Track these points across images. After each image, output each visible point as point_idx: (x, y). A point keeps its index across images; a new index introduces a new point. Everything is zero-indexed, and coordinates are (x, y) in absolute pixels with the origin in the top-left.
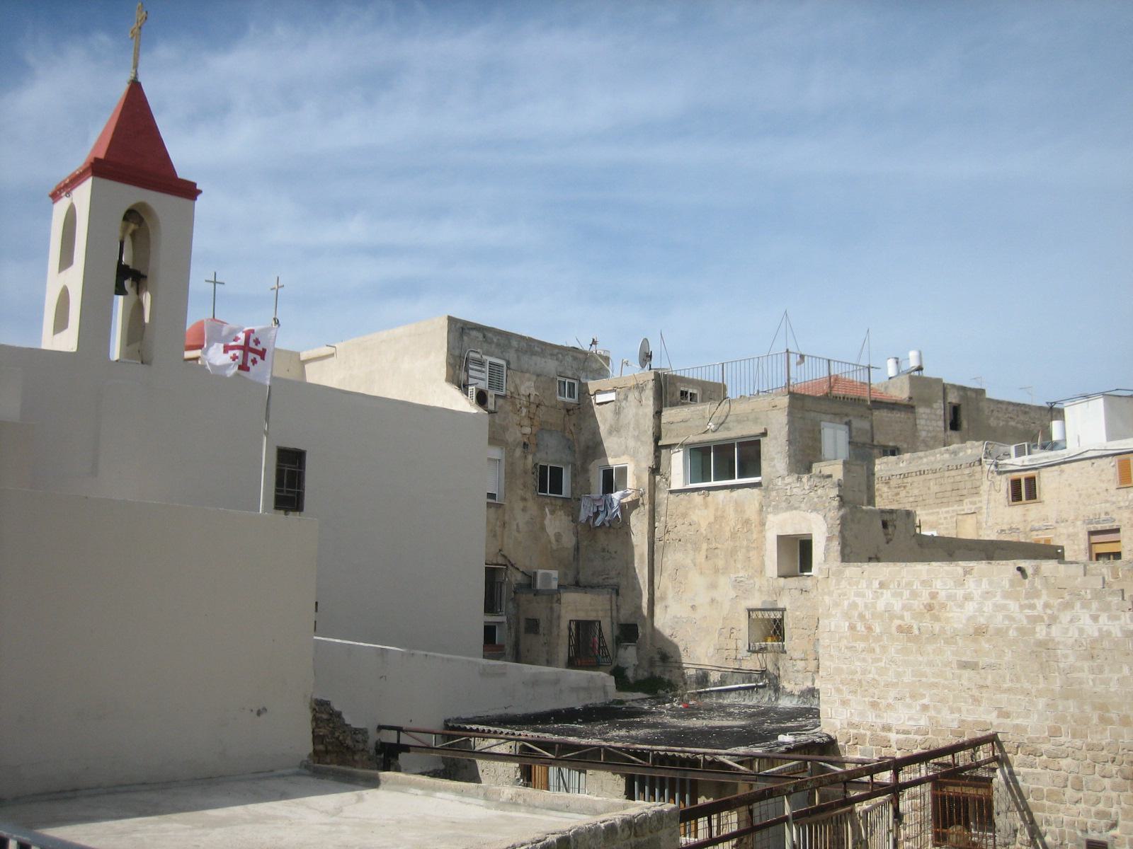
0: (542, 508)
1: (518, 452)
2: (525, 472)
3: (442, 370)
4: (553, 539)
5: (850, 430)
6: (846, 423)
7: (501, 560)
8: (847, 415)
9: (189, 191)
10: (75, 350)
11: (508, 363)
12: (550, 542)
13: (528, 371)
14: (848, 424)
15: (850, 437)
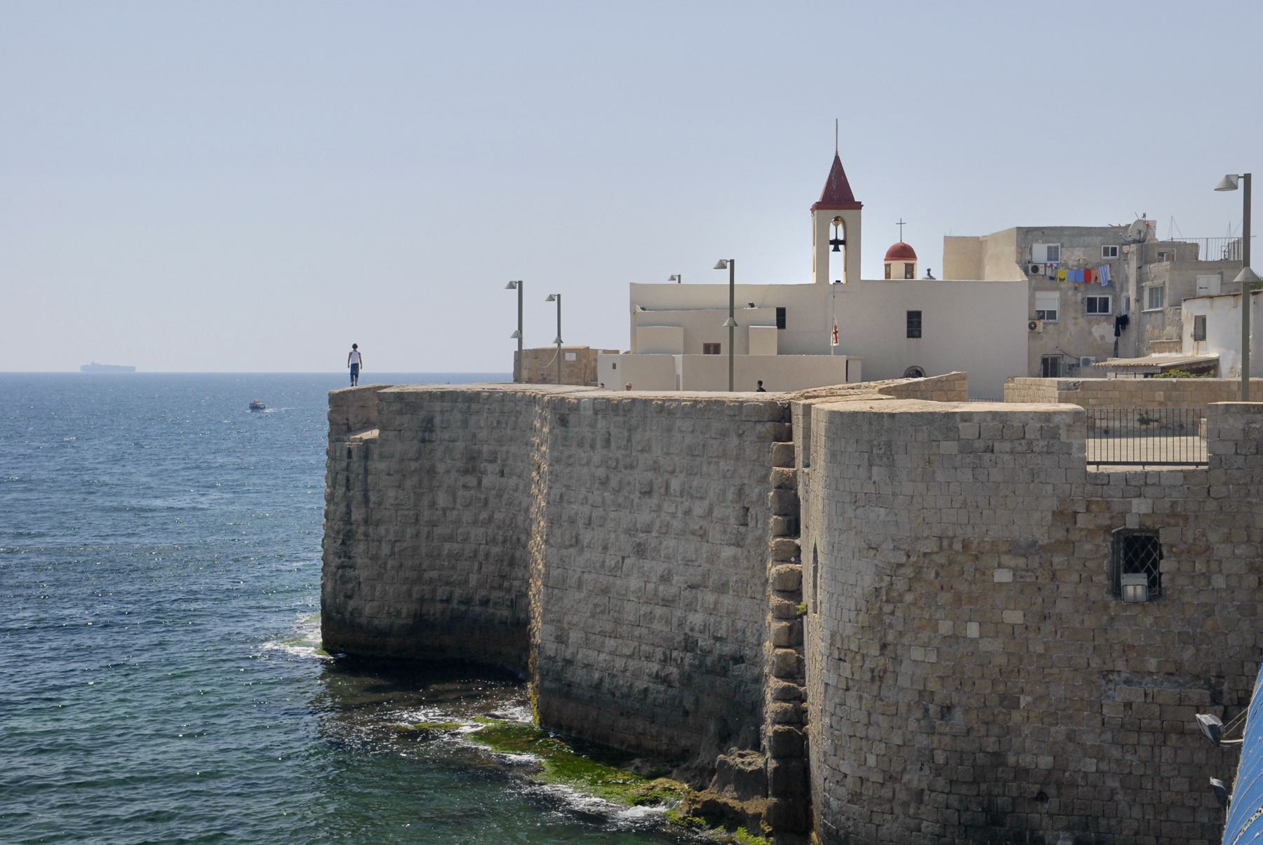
0: (1090, 322)
1: (1070, 293)
2: (1076, 303)
3: (1013, 257)
4: (1098, 339)
5: (1222, 278)
6: (1219, 273)
7: (1058, 352)
8: (1219, 269)
9: (859, 206)
10: (815, 282)
11: (1062, 246)
12: (1096, 340)
13: (1078, 246)
14: (1221, 273)
15: (1222, 280)
